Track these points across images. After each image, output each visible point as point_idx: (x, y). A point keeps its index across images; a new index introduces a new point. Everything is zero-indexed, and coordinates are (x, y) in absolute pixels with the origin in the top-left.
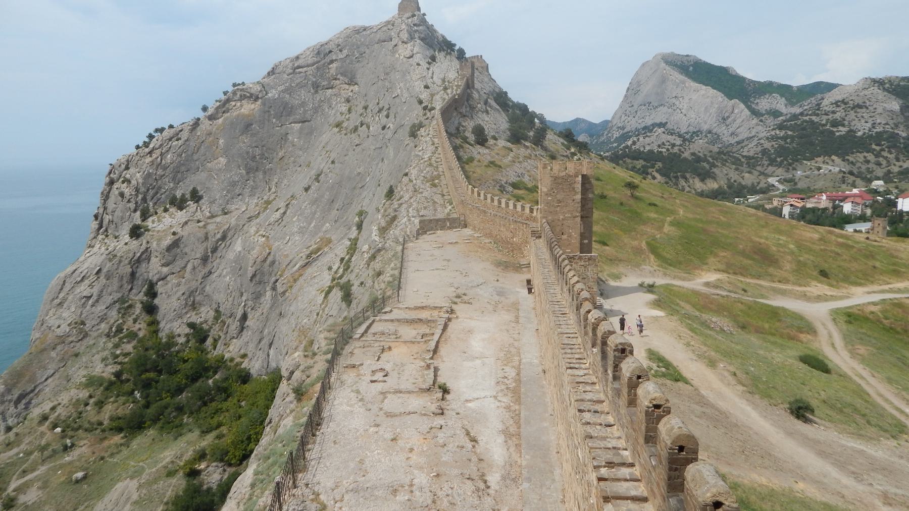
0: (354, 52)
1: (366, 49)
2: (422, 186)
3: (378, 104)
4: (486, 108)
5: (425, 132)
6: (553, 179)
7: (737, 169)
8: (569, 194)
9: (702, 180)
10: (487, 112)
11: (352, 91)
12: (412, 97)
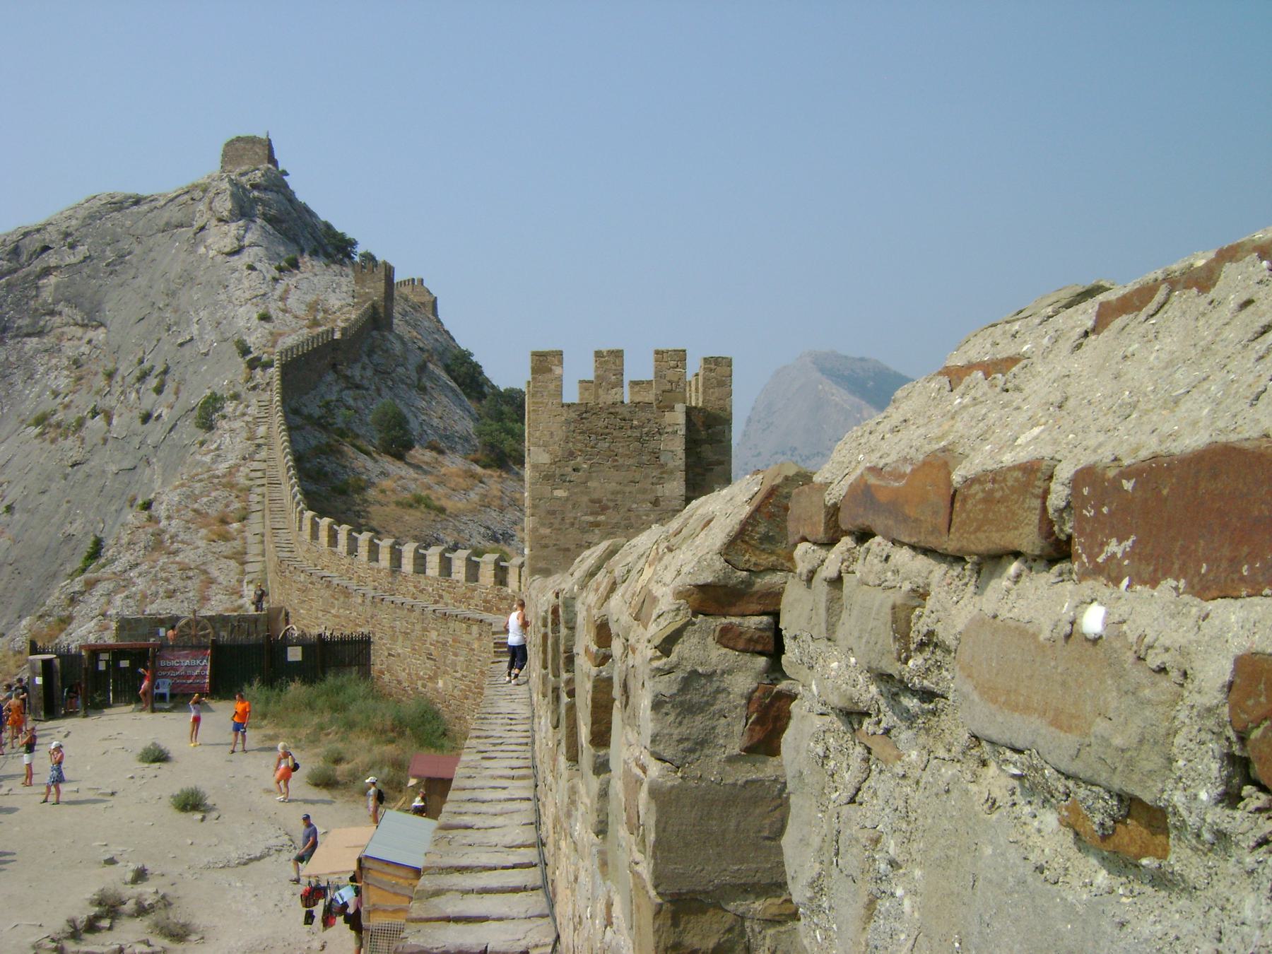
0: (104, 251)
1: (135, 245)
2: (182, 536)
3: (141, 362)
4: (419, 379)
5: (235, 410)
6: (574, 415)
8: (638, 477)
10: (423, 389)
11: (90, 342)
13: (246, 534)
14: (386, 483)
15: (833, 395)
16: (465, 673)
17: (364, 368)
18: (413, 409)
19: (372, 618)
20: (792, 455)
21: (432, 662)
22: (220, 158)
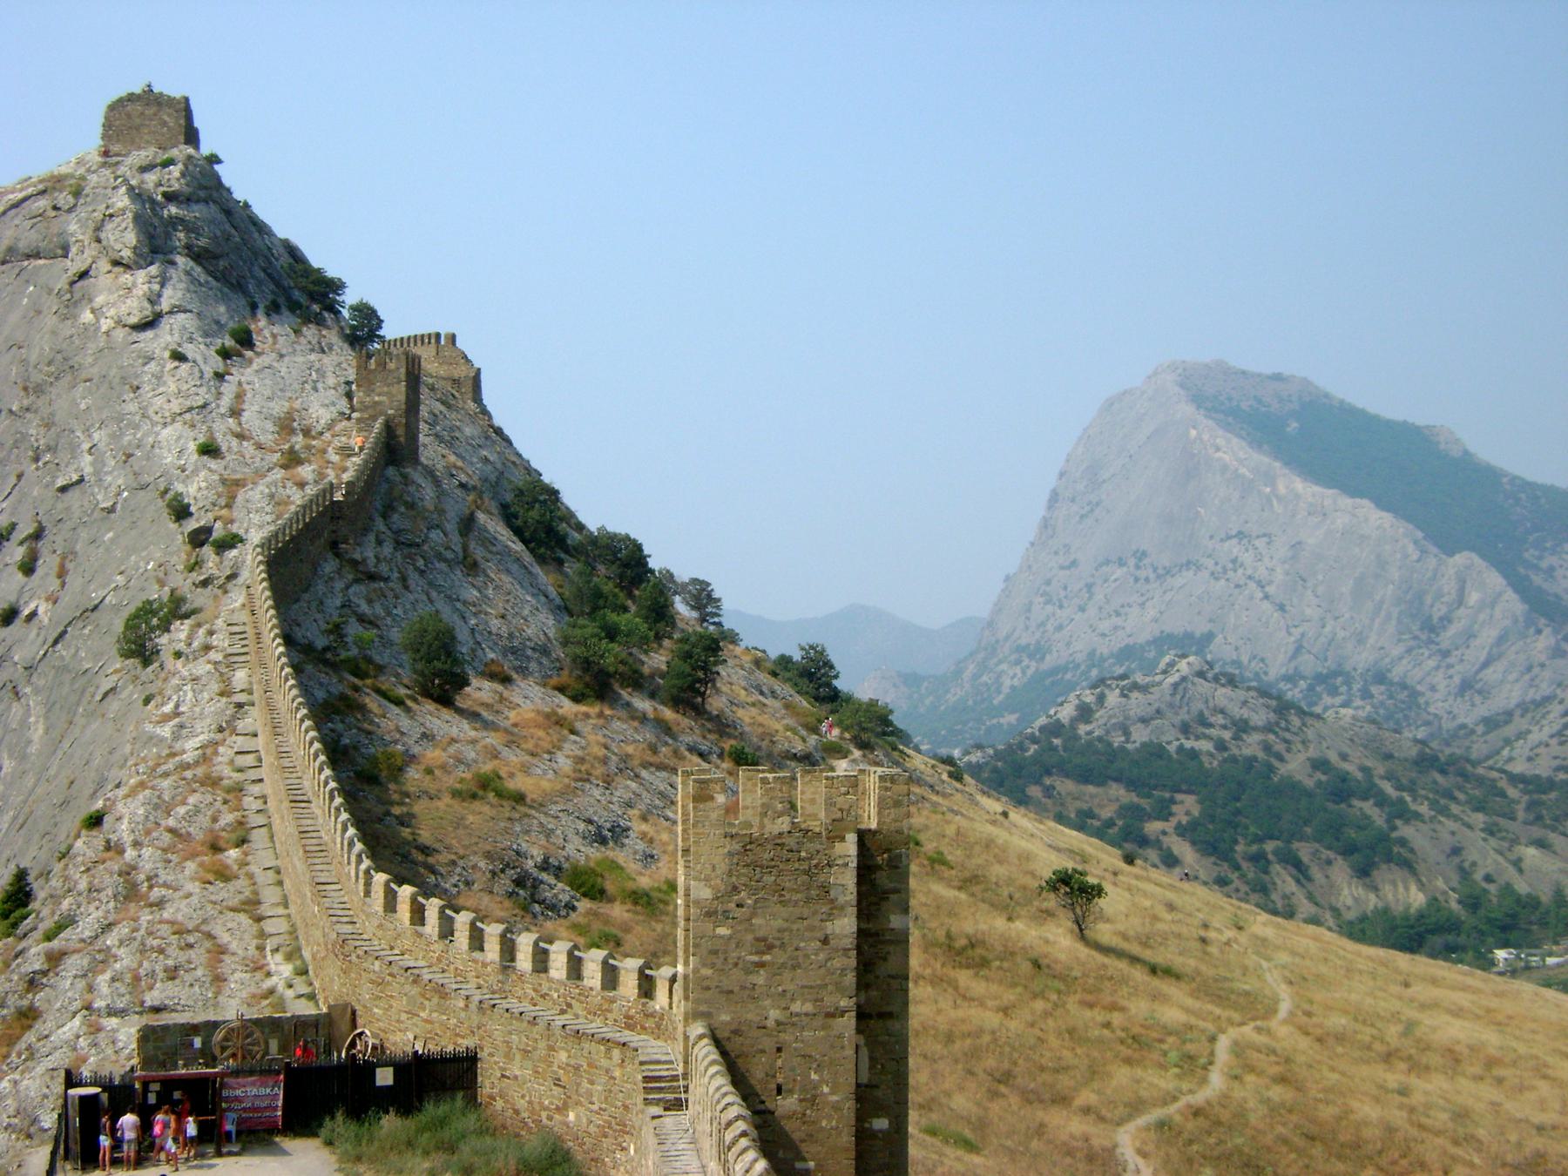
2: (164, 876)
4: (465, 549)
6: (737, 847)
7: (1491, 831)
8: (806, 912)
9: (1363, 872)
12: (144, 487)
13: (253, 868)
14: (433, 755)
15: (1218, 449)
16: (603, 1106)
17: (380, 543)
18: (459, 605)
19: (479, 1028)
20: (1138, 567)
21: (561, 1090)
22: (100, 130)
